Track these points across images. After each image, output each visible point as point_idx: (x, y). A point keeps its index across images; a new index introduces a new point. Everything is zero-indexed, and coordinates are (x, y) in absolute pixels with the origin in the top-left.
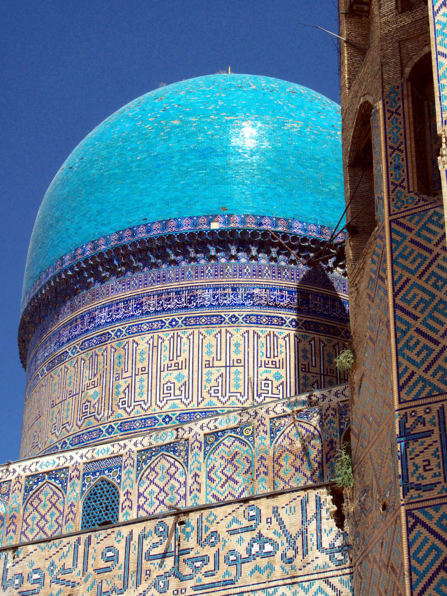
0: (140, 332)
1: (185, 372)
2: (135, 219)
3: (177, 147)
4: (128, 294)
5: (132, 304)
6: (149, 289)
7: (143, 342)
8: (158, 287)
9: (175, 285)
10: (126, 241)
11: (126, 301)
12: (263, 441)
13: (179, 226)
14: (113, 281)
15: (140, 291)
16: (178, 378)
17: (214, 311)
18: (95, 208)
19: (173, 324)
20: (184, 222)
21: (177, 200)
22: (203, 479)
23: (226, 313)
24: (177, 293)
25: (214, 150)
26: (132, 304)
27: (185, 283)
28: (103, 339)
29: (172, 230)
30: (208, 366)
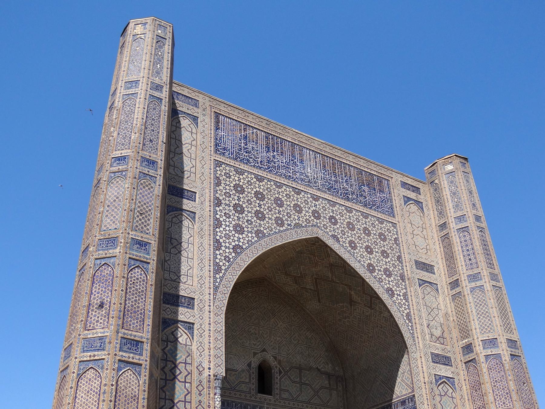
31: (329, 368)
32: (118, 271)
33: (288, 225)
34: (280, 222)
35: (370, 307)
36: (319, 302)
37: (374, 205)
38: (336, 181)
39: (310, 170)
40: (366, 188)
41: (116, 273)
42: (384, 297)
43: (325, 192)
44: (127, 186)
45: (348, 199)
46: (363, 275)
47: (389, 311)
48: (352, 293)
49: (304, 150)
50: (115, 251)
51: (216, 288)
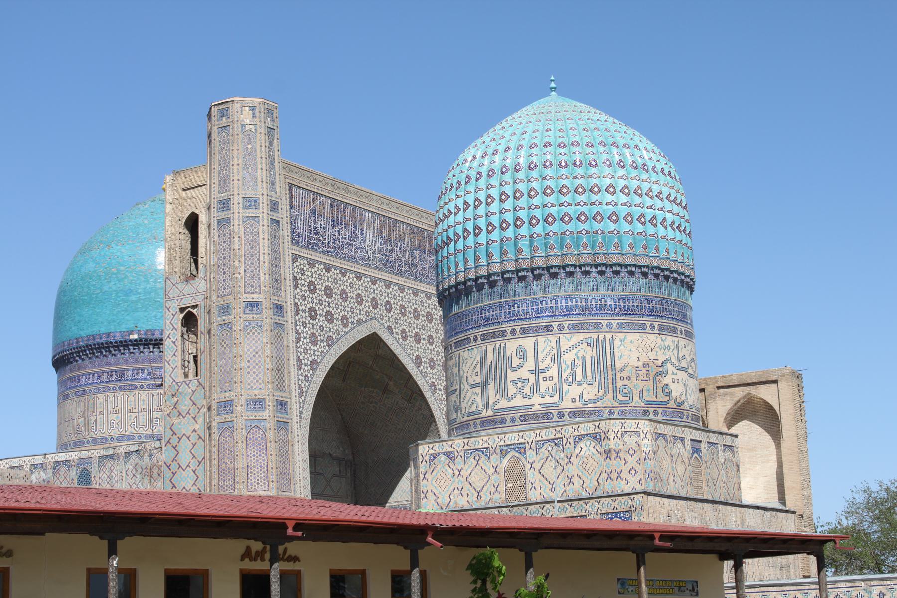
0: (99, 392)
1: (119, 415)
2: (95, 330)
3: (114, 288)
4: (94, 370)
5: (96, 377)
6: (103, 369)
7: (101, 396)
8: (107, 368)
9: (114, 368)
10: (91, 342)
11: (93, 374)
12: (146, 459)
13: (114, 337)
14: (87, 362)
15: (99, 369)
16: (117, 417)
17: (132, 383)
18: (77, 318)
19: (114, 389)
20: (117, 335)
21: (114, 322)
22: (124, 474)
23: (138, 384)
24: (116, 372)
25: (132, 291)
26: (96, 377)
27: (119, 367)
28: (84, 393)
29: (111, 339)
30: (130, 412)
31: (339, 452)
32: (270, 435)
33: (353, 323)
34: (345, 321)
35: (409, 401)
36: (344, 380)
37: (423, 275)
38: (391, 251)
39: (370, 241)
40: (417, 253)
41: (268, 437)
42: (427, 394)
43: (381, 269)
44: (265, 340)
45: (401, 274)
46: (411, 372)
47: (430, 411)
48: (391, 383)
49: (365, 214)
50: (264, 413)
51: (301, 413)
